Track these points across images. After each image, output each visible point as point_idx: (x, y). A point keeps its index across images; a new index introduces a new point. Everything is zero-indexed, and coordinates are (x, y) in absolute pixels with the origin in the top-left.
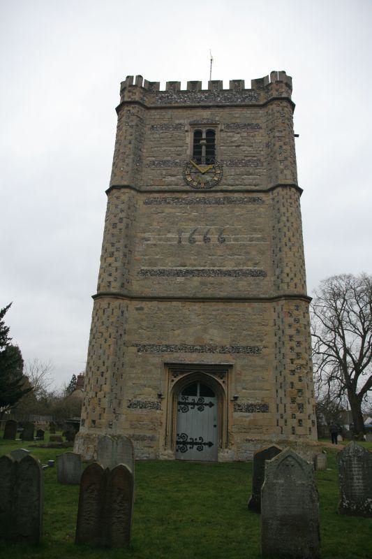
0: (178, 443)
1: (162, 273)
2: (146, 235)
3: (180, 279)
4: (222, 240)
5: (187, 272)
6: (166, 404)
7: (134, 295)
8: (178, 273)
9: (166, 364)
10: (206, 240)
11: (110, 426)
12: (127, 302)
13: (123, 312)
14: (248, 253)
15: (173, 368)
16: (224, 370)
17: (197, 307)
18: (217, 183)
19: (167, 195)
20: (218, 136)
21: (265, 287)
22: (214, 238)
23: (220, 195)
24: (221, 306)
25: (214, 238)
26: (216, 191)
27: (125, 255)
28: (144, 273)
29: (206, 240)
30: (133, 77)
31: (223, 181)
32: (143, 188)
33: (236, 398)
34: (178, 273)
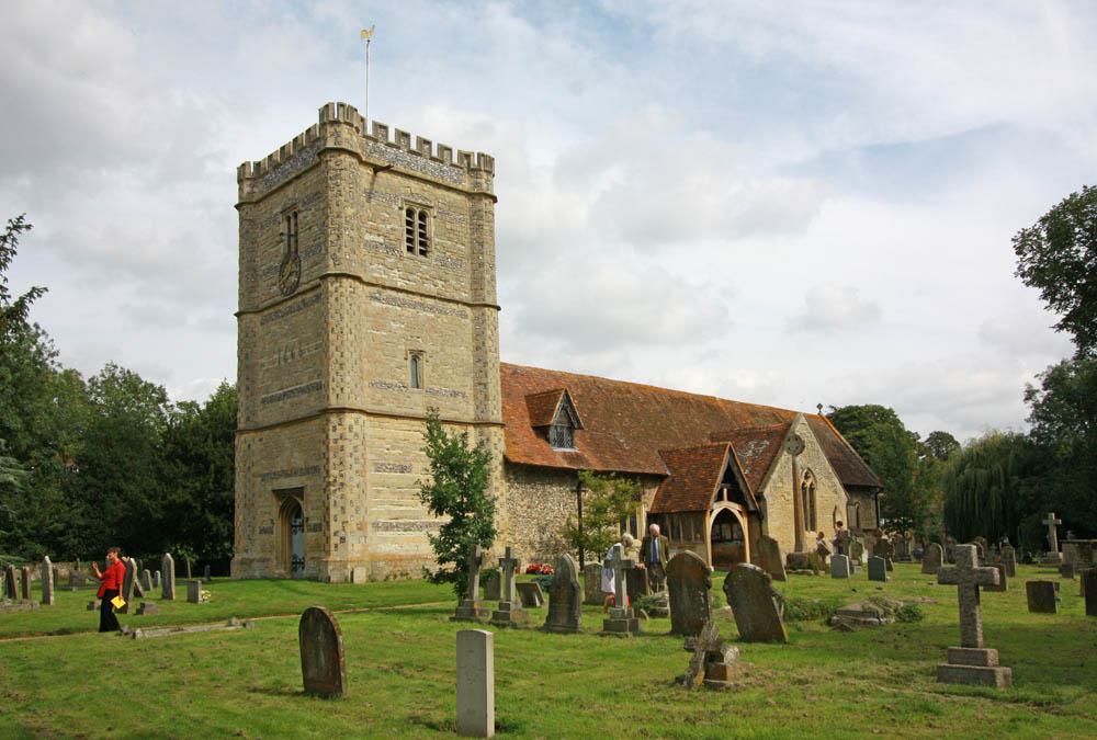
0: (293, 563)
1: (272, 399)
2: (263, 361)
3: (281, 403)
4: (301, 352)
5: (285, 394)
6: (279, 528)
7: (261, 426)
8: (279, 398)
9: (274, 491)
10: (293, 355)
11: (246, 551)
12: (253, 434)
13: (249, 446)
14: (314, 364)
15: (279, 493)
16: (300, 491)
17: (287, 432)
18: (297, 284)
19: (272, 310)
20: (300, 216)
21: (310, 404)
22: (296, 351)
23: (299, 299)
24: (298, 427)
25: (296, 351)
26: (295, 296)
27: (248, 389)
28: (263, 401)
29: (293, 355)
30: (249, 163)
31: (302, 280)
32: (262, 306)
33: (308, 518)
34: (279, 398)
